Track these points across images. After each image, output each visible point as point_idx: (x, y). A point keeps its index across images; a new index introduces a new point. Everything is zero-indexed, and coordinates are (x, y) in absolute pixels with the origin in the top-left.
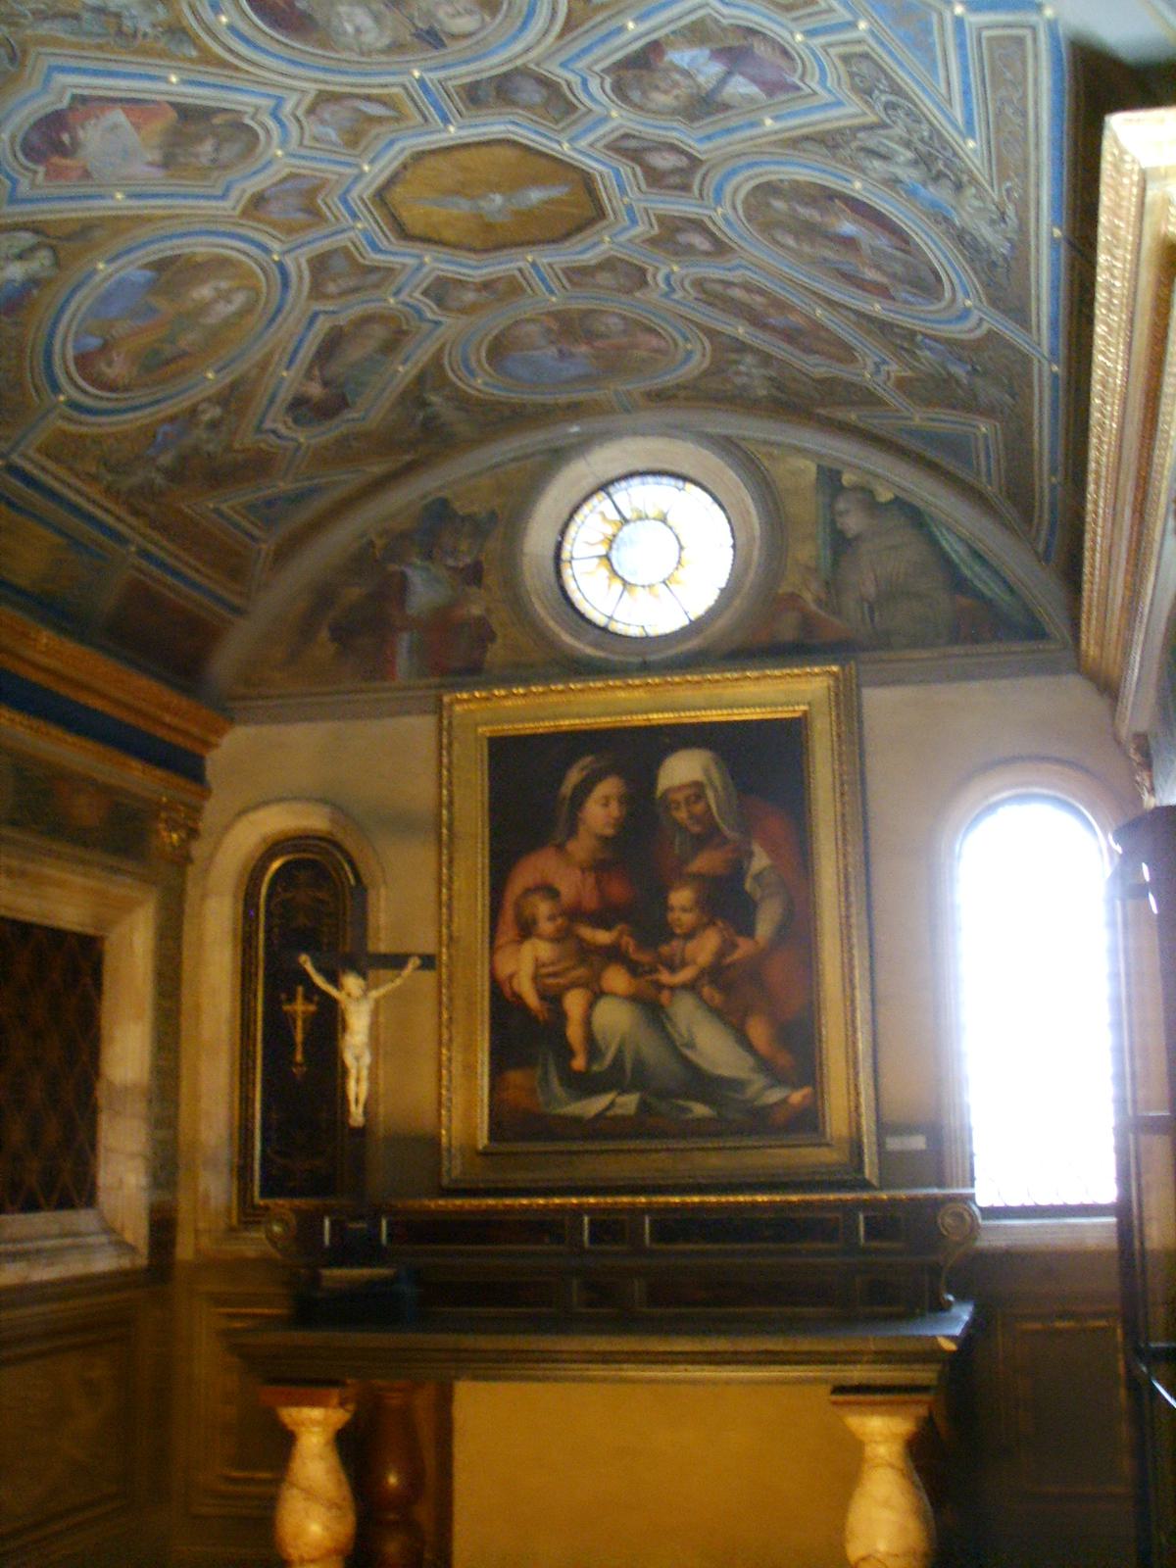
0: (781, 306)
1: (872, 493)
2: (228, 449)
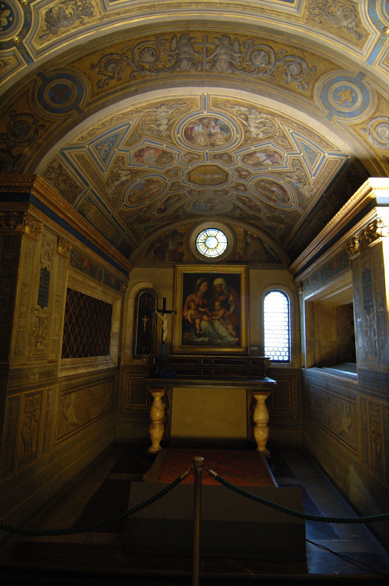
0: (251, 201)
1: (253, 236)
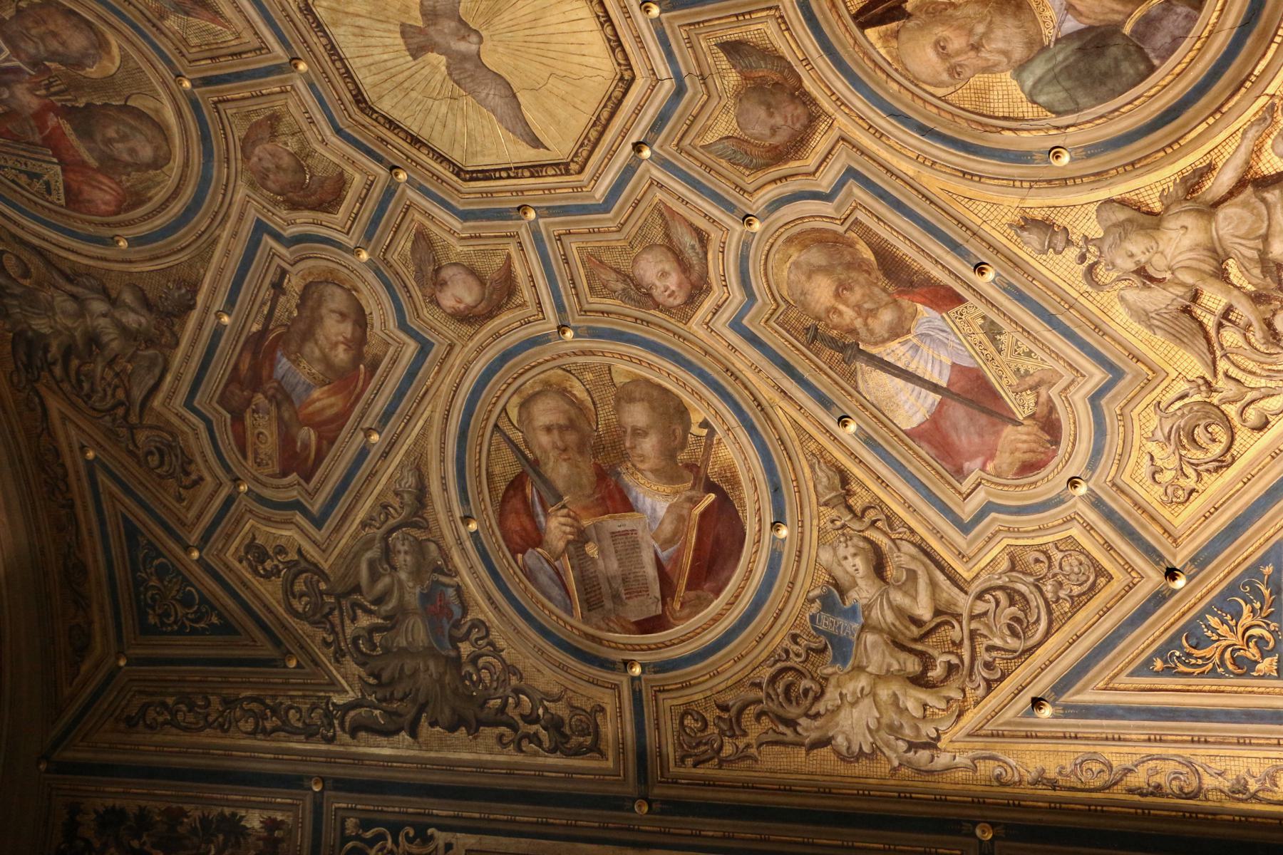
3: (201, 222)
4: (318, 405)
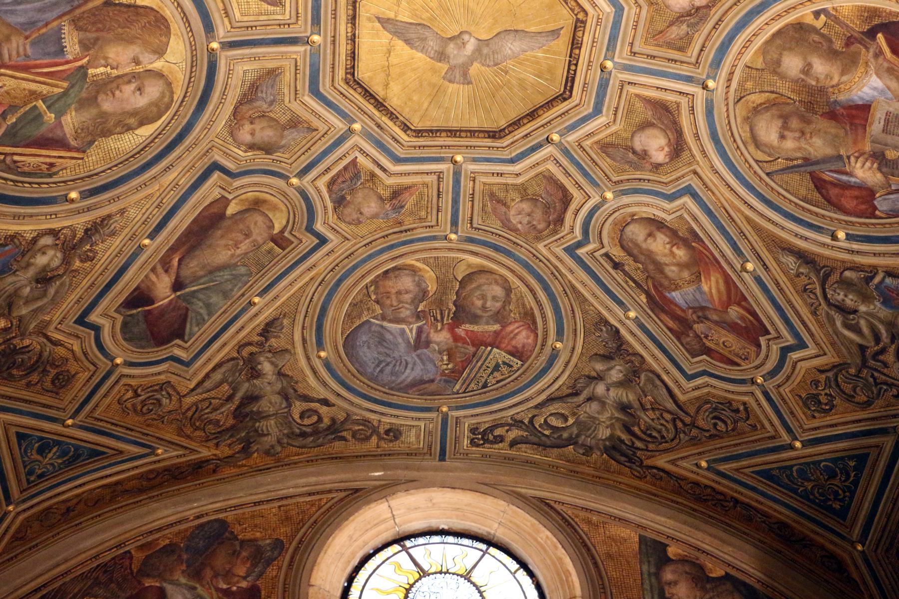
1: (701, 568)
2: (41, 331)
3: (556, 288)
4: (714, 291)
